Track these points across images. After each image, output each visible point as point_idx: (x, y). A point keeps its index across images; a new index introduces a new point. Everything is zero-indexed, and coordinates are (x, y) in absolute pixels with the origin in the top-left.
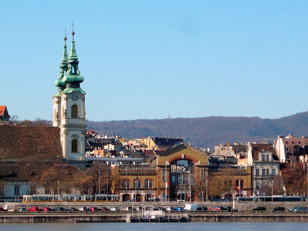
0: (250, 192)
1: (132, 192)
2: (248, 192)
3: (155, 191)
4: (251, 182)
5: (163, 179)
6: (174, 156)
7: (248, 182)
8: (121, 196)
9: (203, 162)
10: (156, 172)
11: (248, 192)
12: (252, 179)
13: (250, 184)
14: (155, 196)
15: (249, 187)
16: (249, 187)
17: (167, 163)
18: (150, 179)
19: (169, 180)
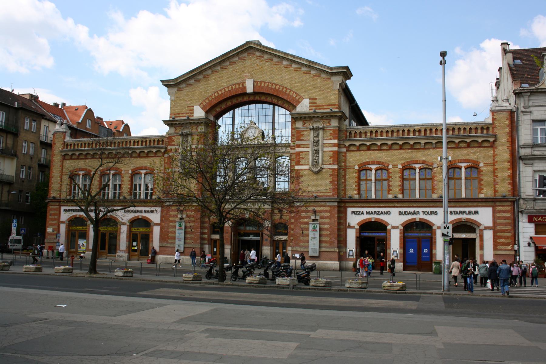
0: (504, 212)
2: (500, 211)
3: (159, 209)
4: (510, 172)
6: (220, 88)
7: (498, 173)
8: (63, 222)
9: (319, 102)
11: (500, 211)
12: (515, 160)
13: (509, 180)
14: (157, 224)
15: (504, 191)
16: (504, 191)
17: (199, 113)
18: (145, 168)
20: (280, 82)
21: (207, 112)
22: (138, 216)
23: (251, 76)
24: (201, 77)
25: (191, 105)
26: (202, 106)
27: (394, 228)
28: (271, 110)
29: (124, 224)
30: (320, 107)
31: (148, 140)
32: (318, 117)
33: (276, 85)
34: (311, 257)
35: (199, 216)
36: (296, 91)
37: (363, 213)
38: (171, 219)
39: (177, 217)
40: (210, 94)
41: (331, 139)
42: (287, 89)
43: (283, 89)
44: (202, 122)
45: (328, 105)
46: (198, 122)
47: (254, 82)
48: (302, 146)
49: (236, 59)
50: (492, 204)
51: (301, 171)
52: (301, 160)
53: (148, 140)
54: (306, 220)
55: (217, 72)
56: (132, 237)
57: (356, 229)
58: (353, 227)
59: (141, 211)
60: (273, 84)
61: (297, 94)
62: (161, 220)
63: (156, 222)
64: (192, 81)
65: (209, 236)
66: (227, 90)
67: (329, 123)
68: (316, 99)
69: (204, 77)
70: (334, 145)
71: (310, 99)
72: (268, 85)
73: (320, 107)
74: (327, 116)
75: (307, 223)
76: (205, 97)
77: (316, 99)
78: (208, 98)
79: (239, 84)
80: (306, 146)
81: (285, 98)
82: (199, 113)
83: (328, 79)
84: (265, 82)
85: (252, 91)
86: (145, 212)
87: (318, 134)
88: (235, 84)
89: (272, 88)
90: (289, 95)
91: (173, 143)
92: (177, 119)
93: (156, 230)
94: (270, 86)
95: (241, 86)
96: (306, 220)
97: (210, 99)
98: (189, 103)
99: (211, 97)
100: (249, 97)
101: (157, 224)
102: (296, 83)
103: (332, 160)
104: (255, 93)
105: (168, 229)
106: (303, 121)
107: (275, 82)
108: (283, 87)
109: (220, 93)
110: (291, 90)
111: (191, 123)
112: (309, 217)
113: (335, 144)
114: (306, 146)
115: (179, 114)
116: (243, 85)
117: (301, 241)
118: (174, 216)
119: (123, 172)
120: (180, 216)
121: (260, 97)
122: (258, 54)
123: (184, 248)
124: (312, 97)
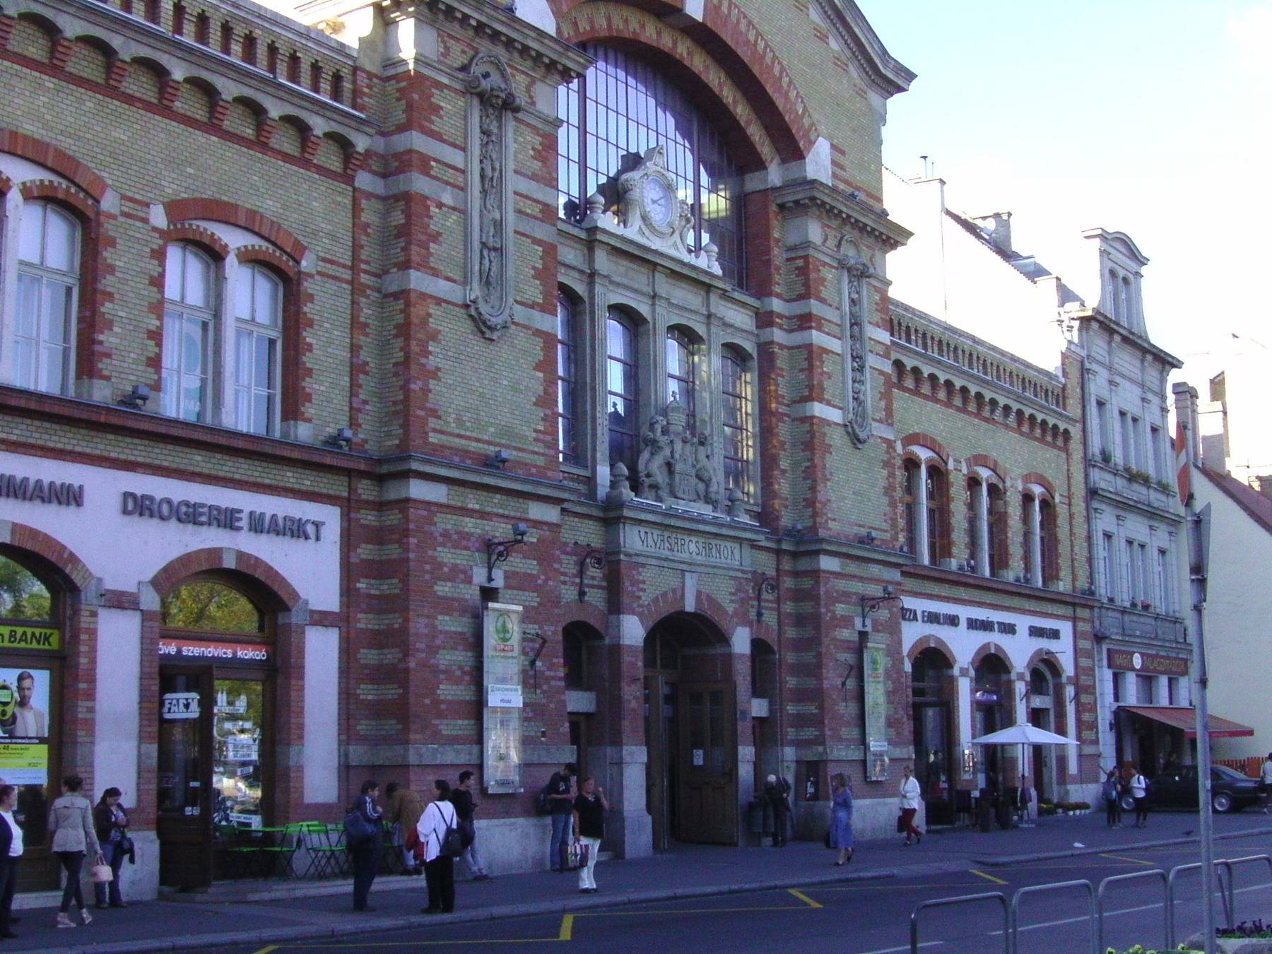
14: (322, 619)
29: (120, 601)
39: (469, 581)
50: (1068, 611)
59: (227, 519)
62: (347, 591)
63: (316, 605)
83: (861, 94)
86: (258, 525)
90: (787, 97)
101: (322, 619)
105: (433, 650)
120: (479, 576)
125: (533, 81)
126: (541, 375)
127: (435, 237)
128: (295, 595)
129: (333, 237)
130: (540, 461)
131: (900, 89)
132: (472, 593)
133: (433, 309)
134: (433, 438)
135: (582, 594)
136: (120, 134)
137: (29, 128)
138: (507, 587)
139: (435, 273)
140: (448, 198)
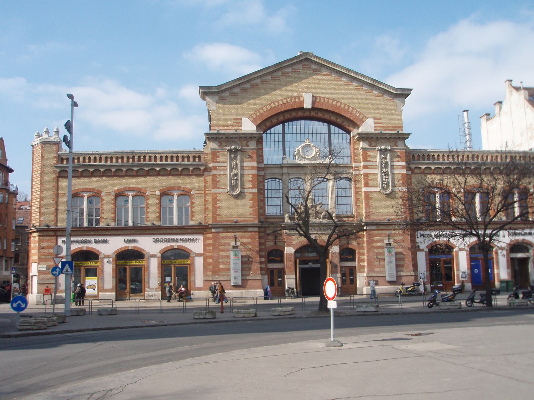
1: (106, 242)
3: (201, 237)
5: (233, 188)
6: (272, 100)
9: (384, 123)
10: (203, 162)
14: (199, 255)
17: (248, 126)
18: (179, 189)
19: (255, 190)
20: (340, 99)
21: (258, 126)
22: (173, 246)
23: (308, 90)
24: (248, 86)
25: (238, 117)
26: (252, 119)
27: (461, 249)
28: (326, 128)
29: (153, 256)
30: (385, 128)
31: (180, 156)
32: (386, 138)
33: (337, 102)
34: (388, 282)
35: (257, 243)
36: (359, 110)
37: (431, 236)
38: (221, 247)
39: (229, 245)
40: (261, 106)
41: (398, 161)
42: (349, 106)
43: (345, 106)
44: (255, 137)
45: (393, 127)
46: (249, 137)
47: (313, 96)
48: (370, 167)
49: (289, 70)
51: (370, 193)
52: (369, 182)
53: (180, 156)
54: (379, 244)
55: (266, 82)
56: (165, 270)
57: (426, 252)
58: (423, 250)
60: (333, 100)
61: (360, 114)
62: (204, 249)
64: (237, 90)
65: (266, 266)
66: (281, 103)
67: (395, 144)
68: (381, 119)
69: (252, 86)
70: (403, 167)
71: (374, 119)
72: (328, 101)
73: (385, 128)
74: (395, 138)
75: (382, 248)
76: (255, 109)
77: (381, 119)
78: (258, 111)
79: (295, 97)
80: (374, 167)
81: (348, 116)
82: (248, 126)
84: (324, 98)
85: (310, 106)
86: (183, 240)
87: (386, 156)
88: (291, 98)
89: (333, 105)
90: (351, 113)
91: (218, 159)
92: (221, 132)
93: (199, 262)
94: (330, 102)
95: (297, 100)
96: (379, 244)
97: (261, 111)
98: (235, 115)
99: (262, 109)
100: (304, 113)
101: (199, 255)
102: (358, 101)
103: (401, 182)
104: (313, 109)
105: (218, 259)
106: (369, 141)
107: (336, 99)
108: (345, 105)
109: (273, 105)
110: (353, 109)
111: (240, 137)
112: (381, 241)
113: (403, 166)
114: (374, 167)
115: (224, 126)
116: (299, 99)
117: (376, 266)
118: (225, 244)
119: (148, 193)
121: (316, 113)
122: (314, 67)
123: (242, 280)
124: (376, 118)
125: (248, 142)
126: (251, 202)
127: (219, 181)
128: (191, 251)
129: (199, 186)
130: (252, 219)
131: (408, 95)
132: (230, 247)
133: (218, 195)
134: (218, 219)
135: (276, 244)
136: (149, 182)
137: (131, 186)
138: (241, 245)
139: (219, 188)
140: (222, 173)
